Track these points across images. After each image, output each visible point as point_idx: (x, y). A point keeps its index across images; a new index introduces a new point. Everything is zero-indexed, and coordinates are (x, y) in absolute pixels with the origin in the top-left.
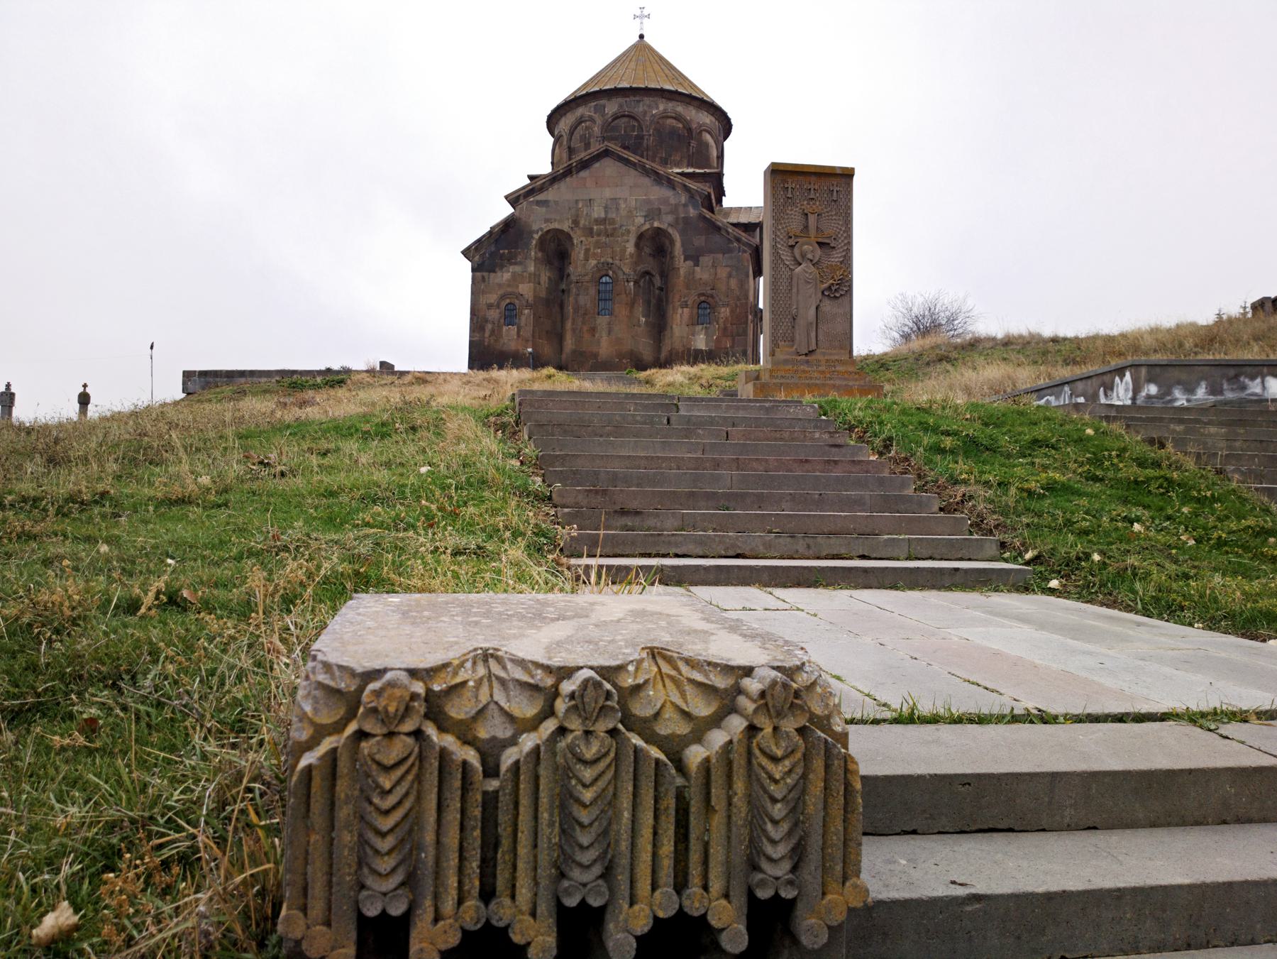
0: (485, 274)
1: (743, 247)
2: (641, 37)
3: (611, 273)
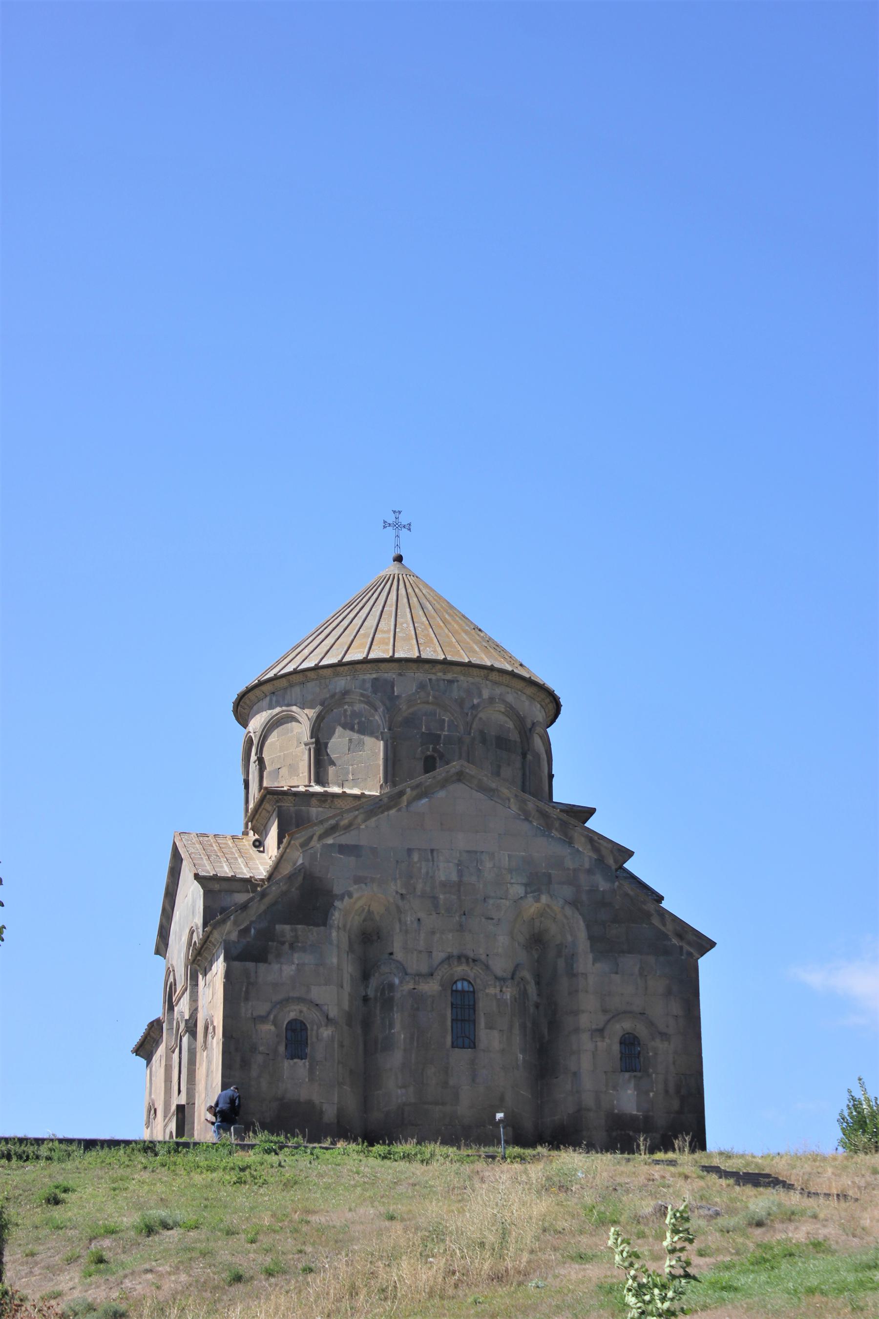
0: (251, 965)
1: (687, 948)
2: (399, 559)
3: (471, 975)
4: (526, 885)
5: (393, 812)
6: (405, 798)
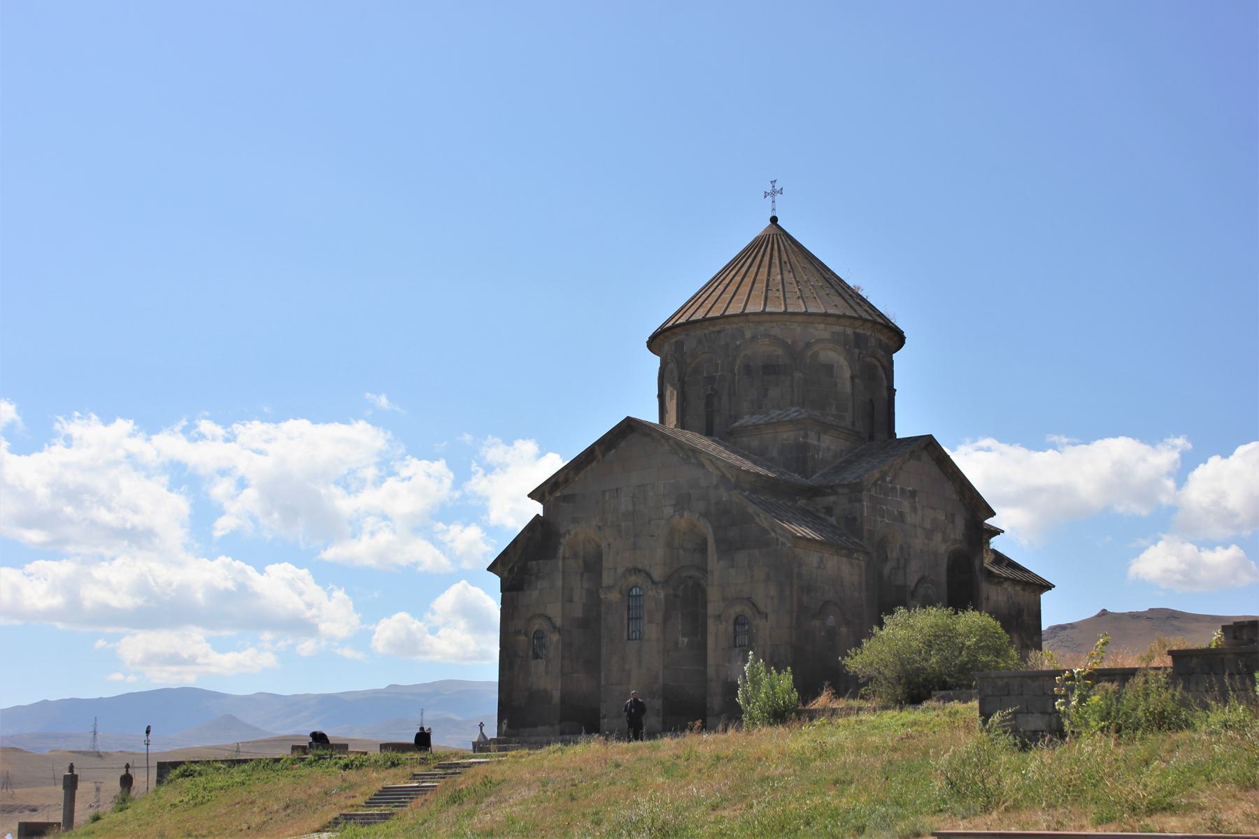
0: (514, 593)
2: (774, 220)
4: (674, 506)
5: (594, 464)
6: (597, 452)
